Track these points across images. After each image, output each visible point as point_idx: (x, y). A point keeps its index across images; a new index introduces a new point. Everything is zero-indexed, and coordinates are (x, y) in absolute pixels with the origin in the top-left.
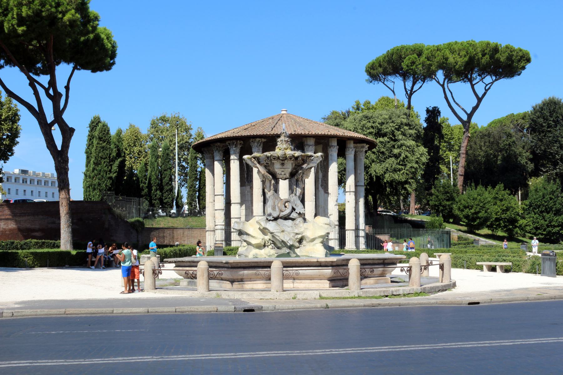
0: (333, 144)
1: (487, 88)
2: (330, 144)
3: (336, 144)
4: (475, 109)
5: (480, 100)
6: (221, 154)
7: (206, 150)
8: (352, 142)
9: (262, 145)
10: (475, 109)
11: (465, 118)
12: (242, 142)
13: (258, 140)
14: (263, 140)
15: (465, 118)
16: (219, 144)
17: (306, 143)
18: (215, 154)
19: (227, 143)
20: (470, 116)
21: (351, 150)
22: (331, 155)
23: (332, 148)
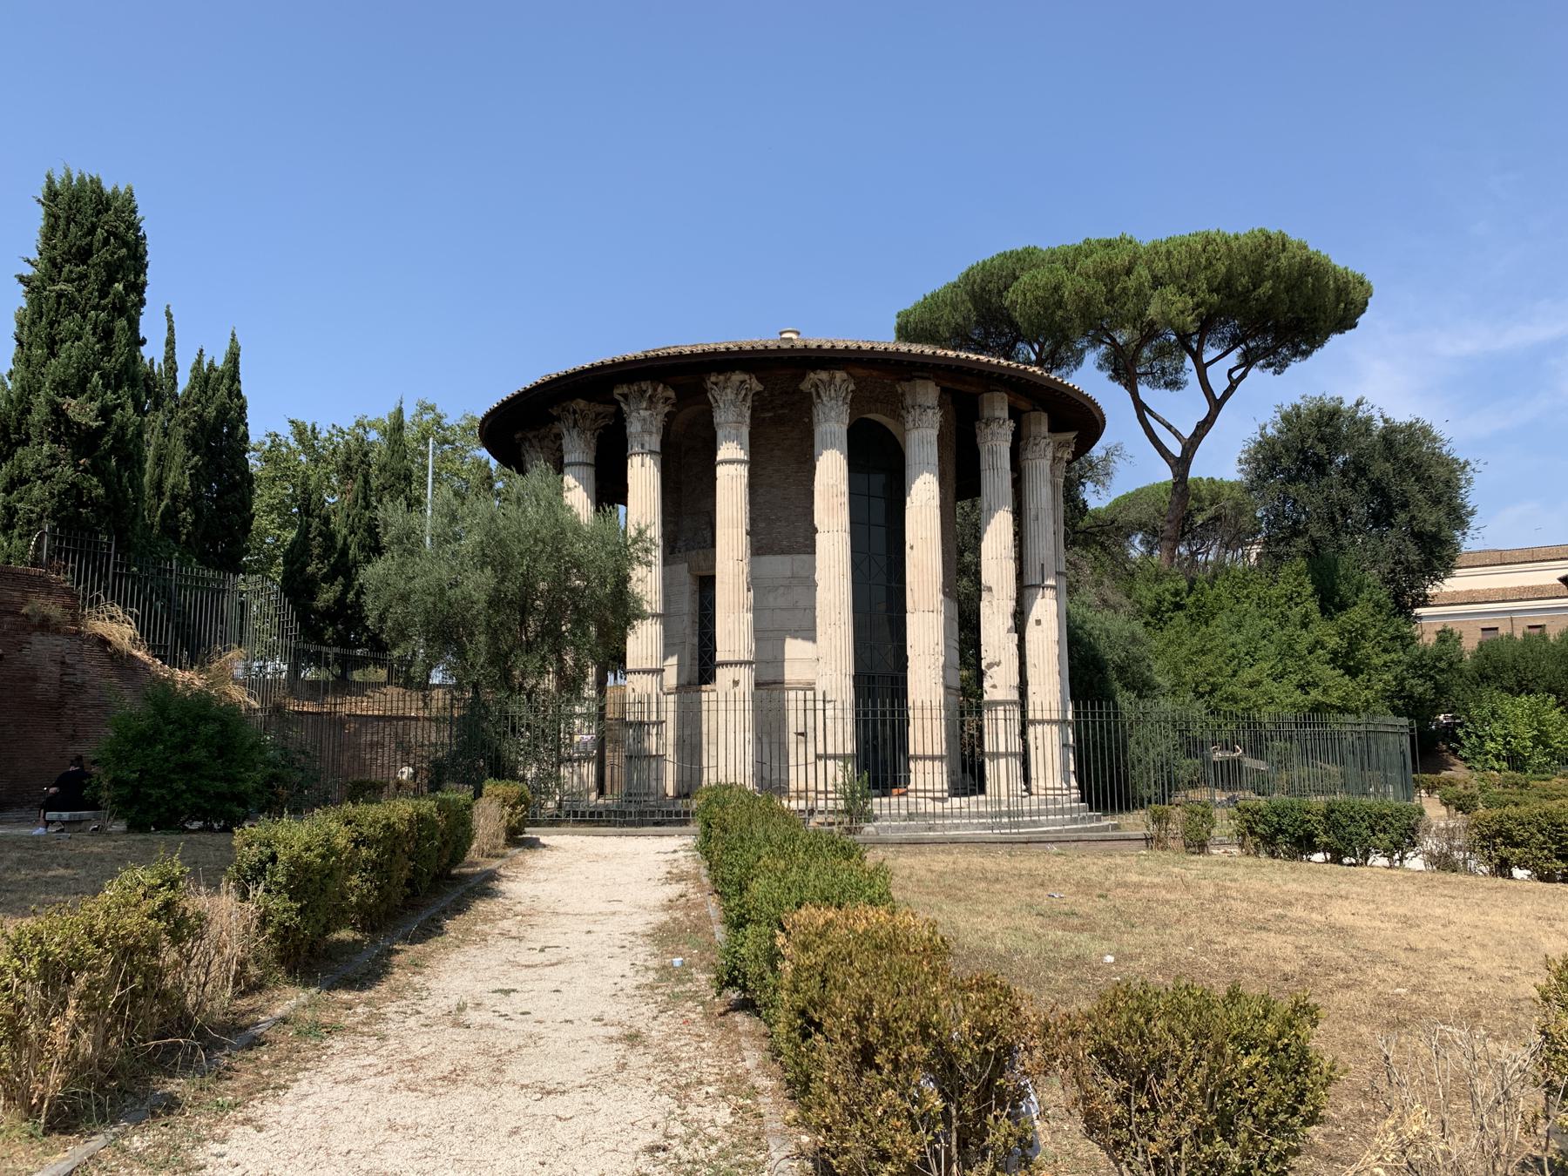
0: (998, 413)
1: (1235, 375)
2: (986, 413)
3: (1006, 414)
4: (1204, 427)
5: (1216, 405)
6: (587, 443)
7: (530, 435)
8: (1044, 418)
9: (749, 404)
10: (1204, 427)
11: (1176, 449)
12: (671, 393)
13: (737, 377)
15: (1176, 449)
16: (581, 404)
17: (909, 401)
18: (567, 443)
19: (617, 393)
20: (1191, 445)
21: (1043, 445)
22: (992, 452)
23: (994, 426)
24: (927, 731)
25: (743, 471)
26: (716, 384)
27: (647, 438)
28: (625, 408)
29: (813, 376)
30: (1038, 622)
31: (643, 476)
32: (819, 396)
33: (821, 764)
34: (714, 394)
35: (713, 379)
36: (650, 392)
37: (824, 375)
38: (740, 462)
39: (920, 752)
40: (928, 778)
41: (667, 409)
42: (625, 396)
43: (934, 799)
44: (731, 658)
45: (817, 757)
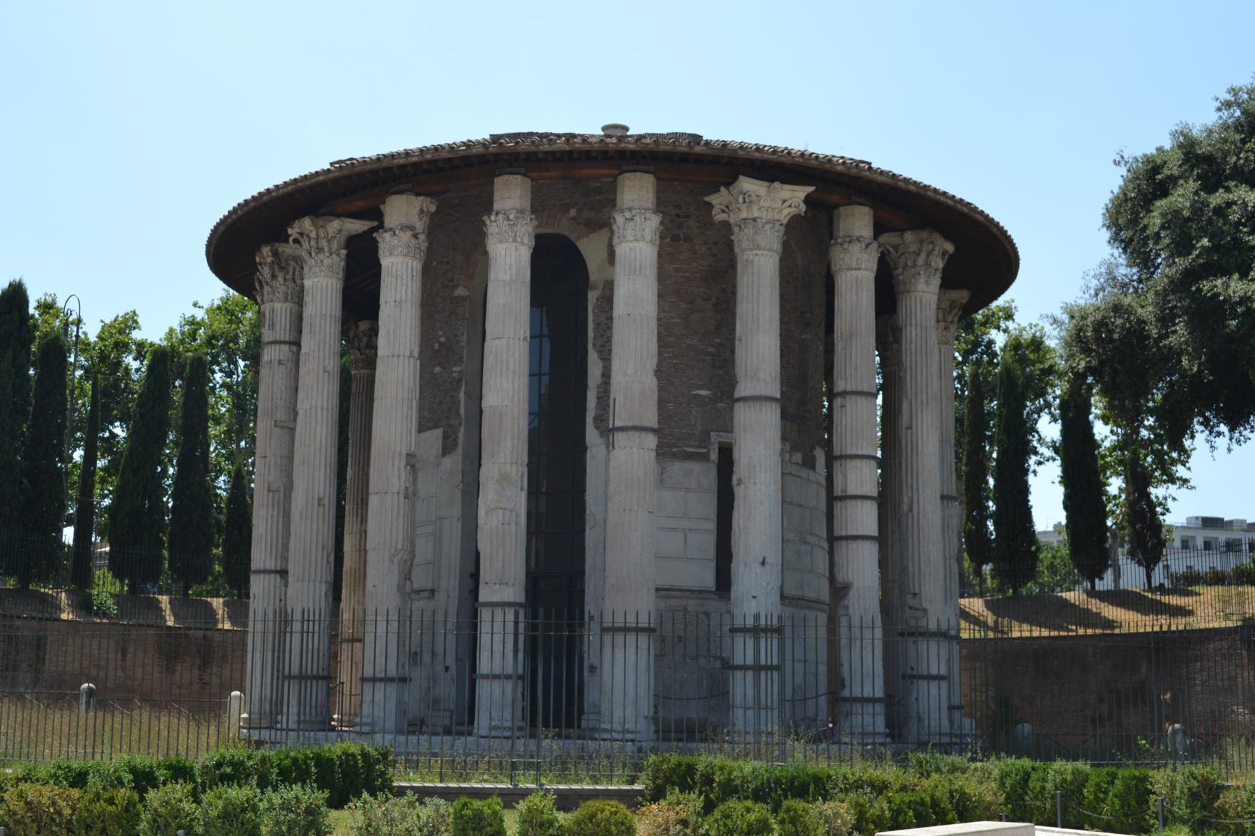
35: (258, 259)
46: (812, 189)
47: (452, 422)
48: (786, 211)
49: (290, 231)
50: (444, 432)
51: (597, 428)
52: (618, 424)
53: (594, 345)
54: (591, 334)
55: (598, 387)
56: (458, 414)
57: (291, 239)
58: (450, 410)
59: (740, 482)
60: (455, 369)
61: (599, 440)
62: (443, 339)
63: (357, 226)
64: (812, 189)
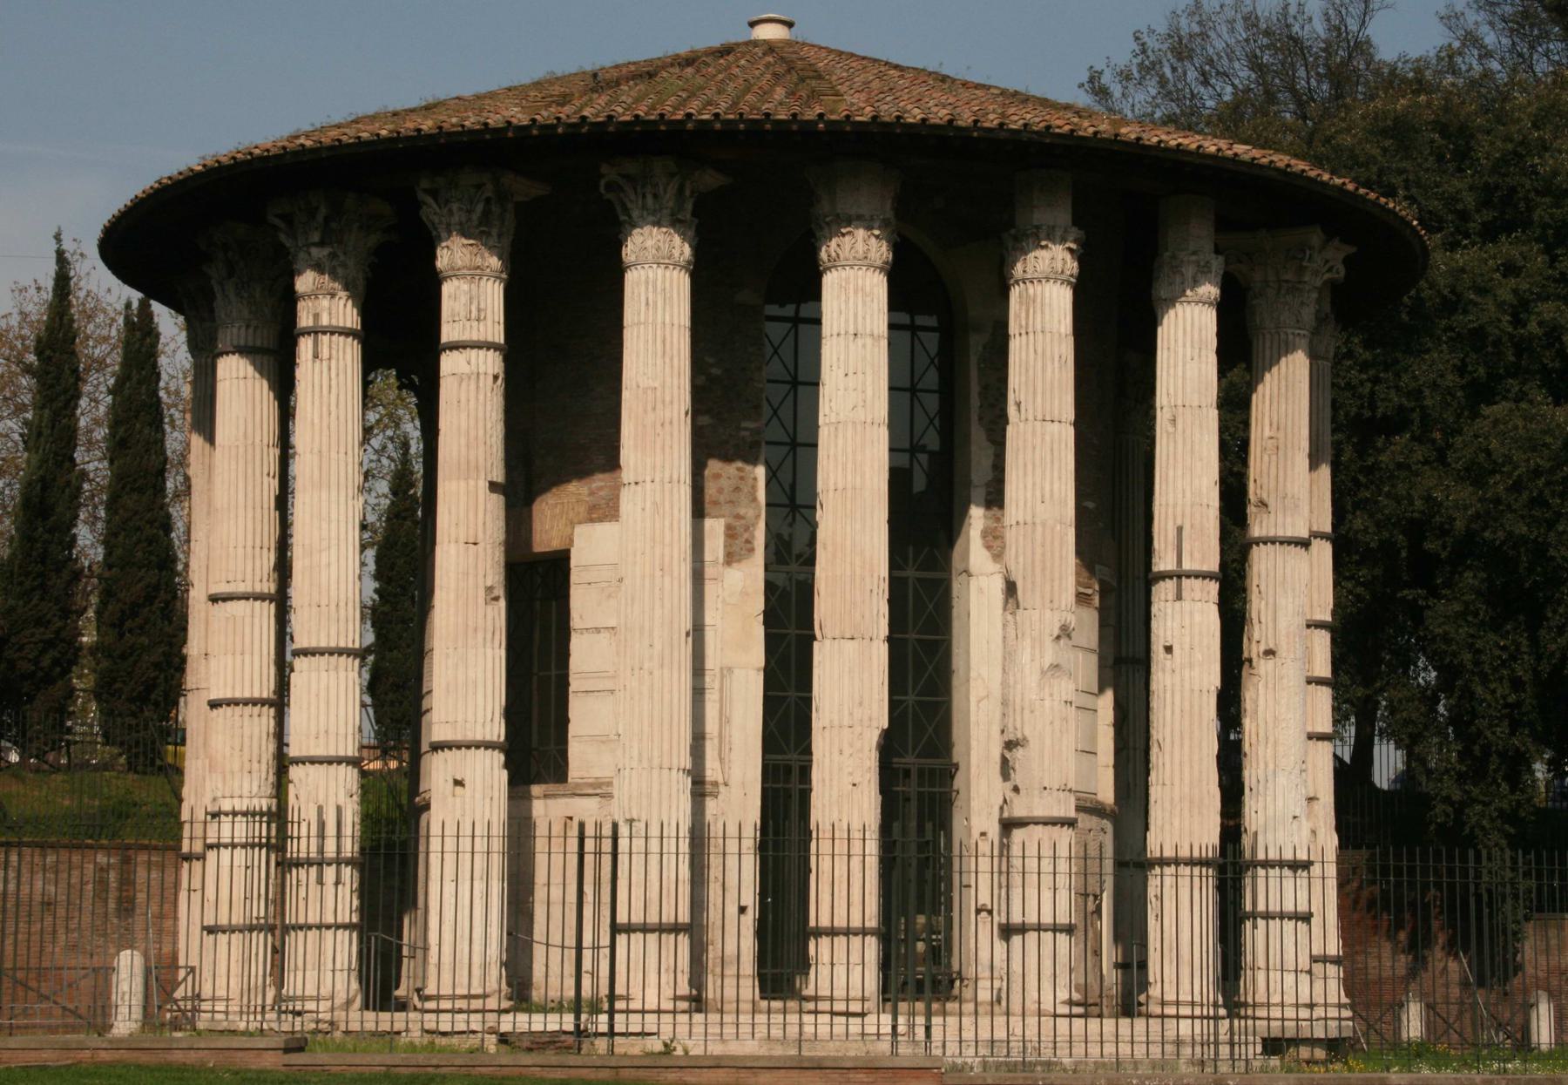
14: (524, 189)
24: (845, 883)
25: (492, 363)
26: (434, 193)
27: (325, 302)
28: (288, 243)
29: (609, 172)
30: (1169, 649)
31: (330, 372)
32: (626, 210)
33: (621, 940)
34: (431, 212)
35: (425, 183)
36: (320, 217)
37: (632, 167)
38: (488, 346)
39: (825, 922)
40: (845, 968)
41: (374, 239)
42: (288, 219)
43: (848, 1014)
44: (459, 737)
45: (616, 929)
46: (1352, 250)
47: (742, 512)
48: (1327, 276)
49: (604, 169)
50: (729, 528)
51: (988, 548)
52: (1187, 565)
53: (981, 419)
54: (975, 402)
55: (988, 485)
56: (755, 499)
57: (603, 182)
58: (737, 489)
59: (1270, 653)
60: (744, 425)
61: (992, 567)
62: (715, 371)
63: (711, 180)
64: (1353, 250)
